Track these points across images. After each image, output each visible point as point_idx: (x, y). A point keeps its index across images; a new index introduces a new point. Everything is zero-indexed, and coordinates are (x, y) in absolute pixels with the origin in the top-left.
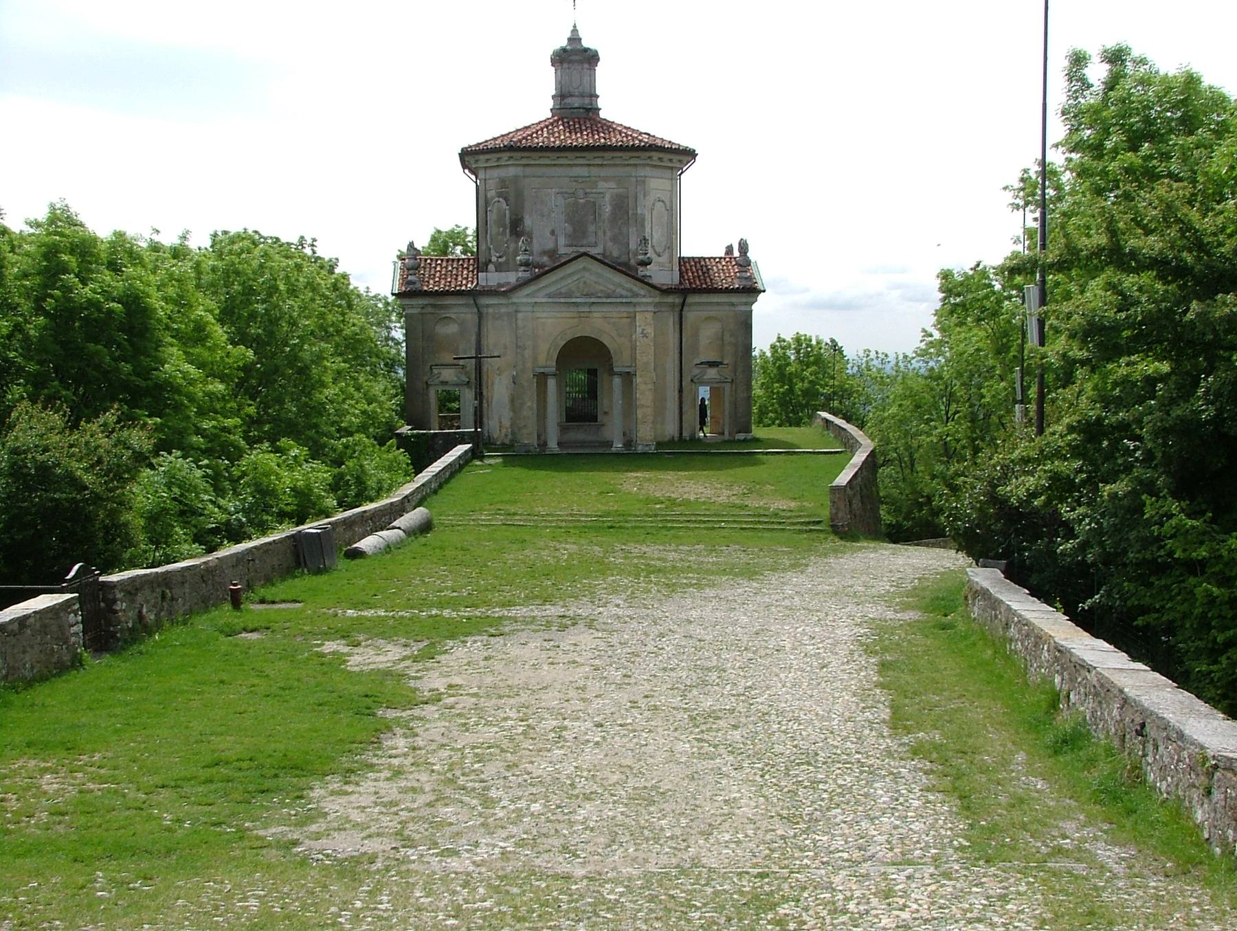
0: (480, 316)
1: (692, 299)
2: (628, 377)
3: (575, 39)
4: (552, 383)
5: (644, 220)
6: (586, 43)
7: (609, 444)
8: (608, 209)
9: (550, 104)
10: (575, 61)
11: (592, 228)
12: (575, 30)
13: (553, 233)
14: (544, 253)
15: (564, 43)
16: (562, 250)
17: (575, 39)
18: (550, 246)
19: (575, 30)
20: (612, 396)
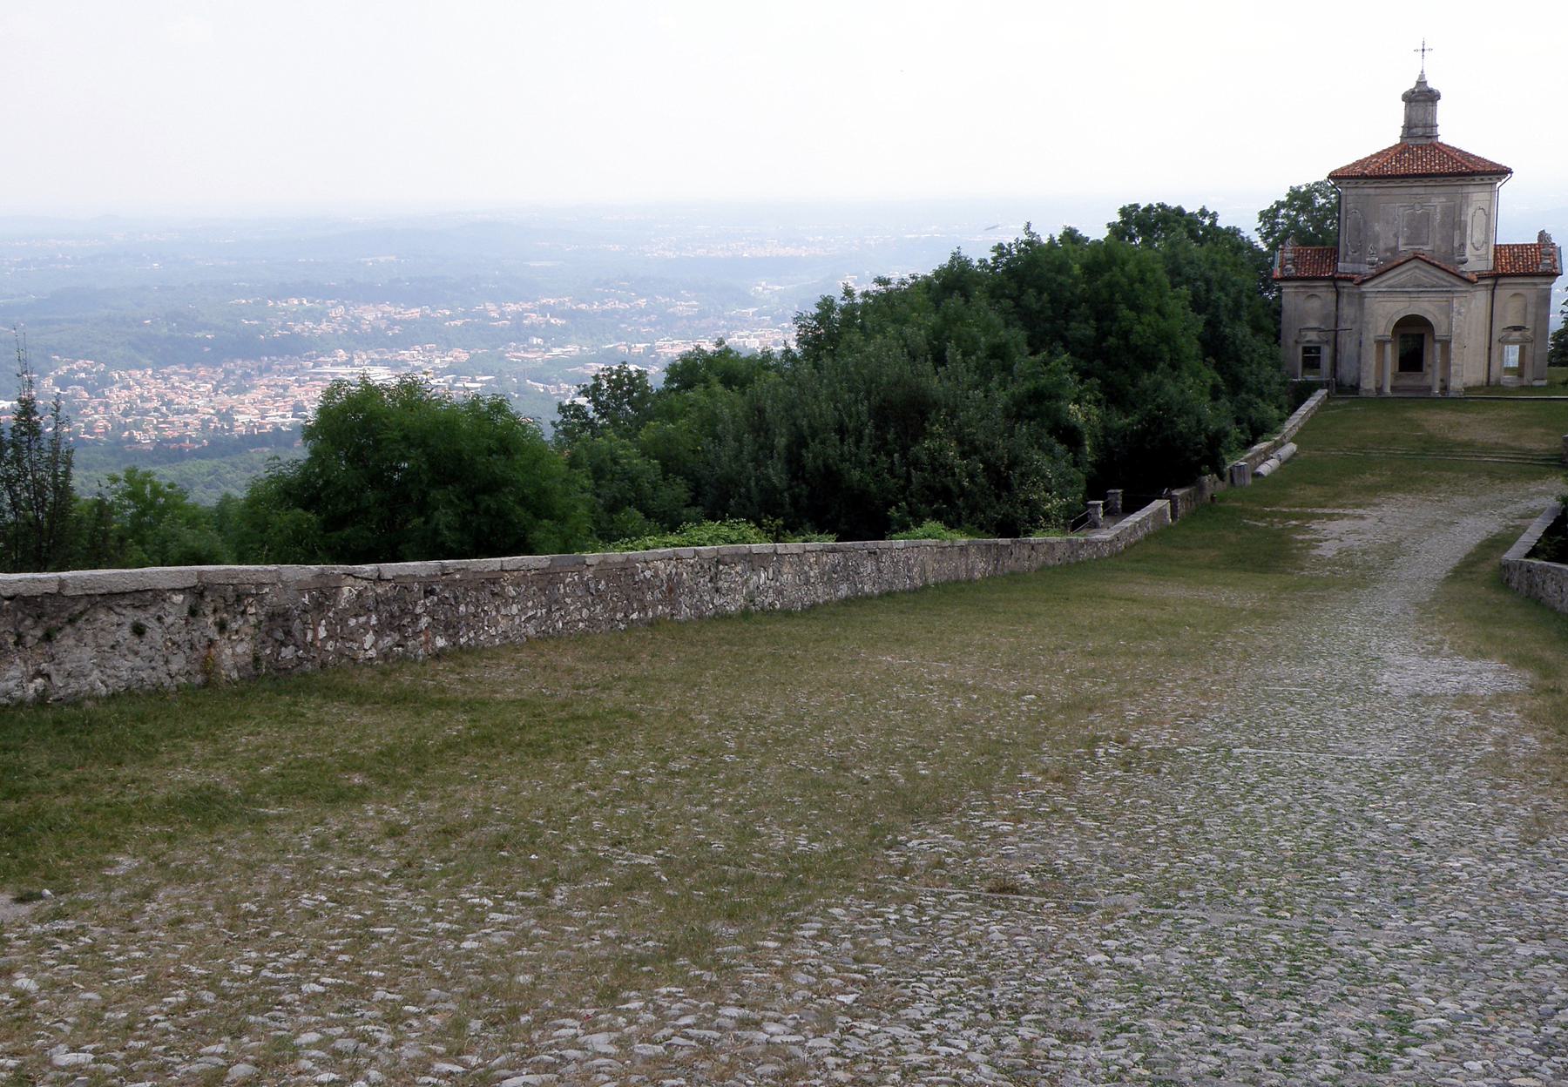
0: (1338, 294)
1: (1501, 281)
2: (1446, 344)
3: (1421, 83)
4: (1389, 347)
6: (1430, 85)
7: (1430, 389)
8: (1438, 217)
9: (1400, 132)
10: (1421, 99)
12: (1422, 75)
13: (1396, 235)
14: (1387, 250)
15: (1412, 85)
17: (1421, 83)
19: (1422, 75)
20: (1433, 355)
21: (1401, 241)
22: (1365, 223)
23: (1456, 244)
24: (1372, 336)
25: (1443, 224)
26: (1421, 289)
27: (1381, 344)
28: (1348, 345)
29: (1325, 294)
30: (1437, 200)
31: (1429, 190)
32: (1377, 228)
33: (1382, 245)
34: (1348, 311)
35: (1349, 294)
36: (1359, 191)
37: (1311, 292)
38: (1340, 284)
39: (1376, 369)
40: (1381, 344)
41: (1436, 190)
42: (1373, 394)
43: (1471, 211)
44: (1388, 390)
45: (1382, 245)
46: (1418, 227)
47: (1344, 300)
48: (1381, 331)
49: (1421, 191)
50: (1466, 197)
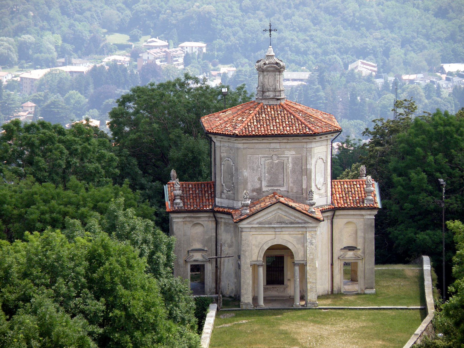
2: (303, 267)
5: (311, 172)
8: (290, 166)
11: (281, 176)
13: (260, 179)
14: (253, 191)
16: (264, 189)
18: (258, 186)
20: (291, 273)
21: (264, 184)
22: (237, 170)
23: (304, 187)
24: (248, 261)
25: (294, 171)
26: (283, 224)
27: (255, 267)
28: (227, 266)
29: (207, 223)
30: (289, 153)
31: (283, 145)
32: (246, 173)
33: (250, 187)
34: (225, 236)
35: (225, 223)
36: (231, 145)
37: (196, 221)
38: (218, 215)
39: (252, 286)
40: (255, 267)
41: (288, 146)
42: (251, 307)
43: (313, 161)
44: (261, 302)
45: (250, 187)
46: (276, 173)
47: (222, 228)
48: (255, 258)
49: (277, 146)
50: (309, 151)
